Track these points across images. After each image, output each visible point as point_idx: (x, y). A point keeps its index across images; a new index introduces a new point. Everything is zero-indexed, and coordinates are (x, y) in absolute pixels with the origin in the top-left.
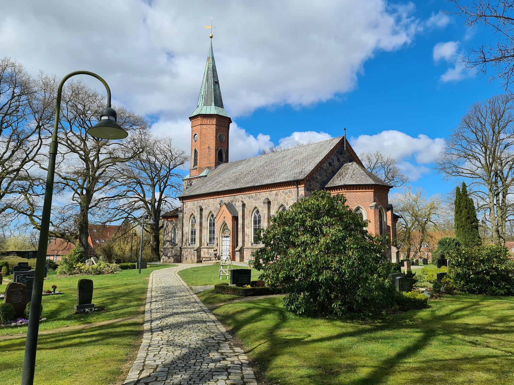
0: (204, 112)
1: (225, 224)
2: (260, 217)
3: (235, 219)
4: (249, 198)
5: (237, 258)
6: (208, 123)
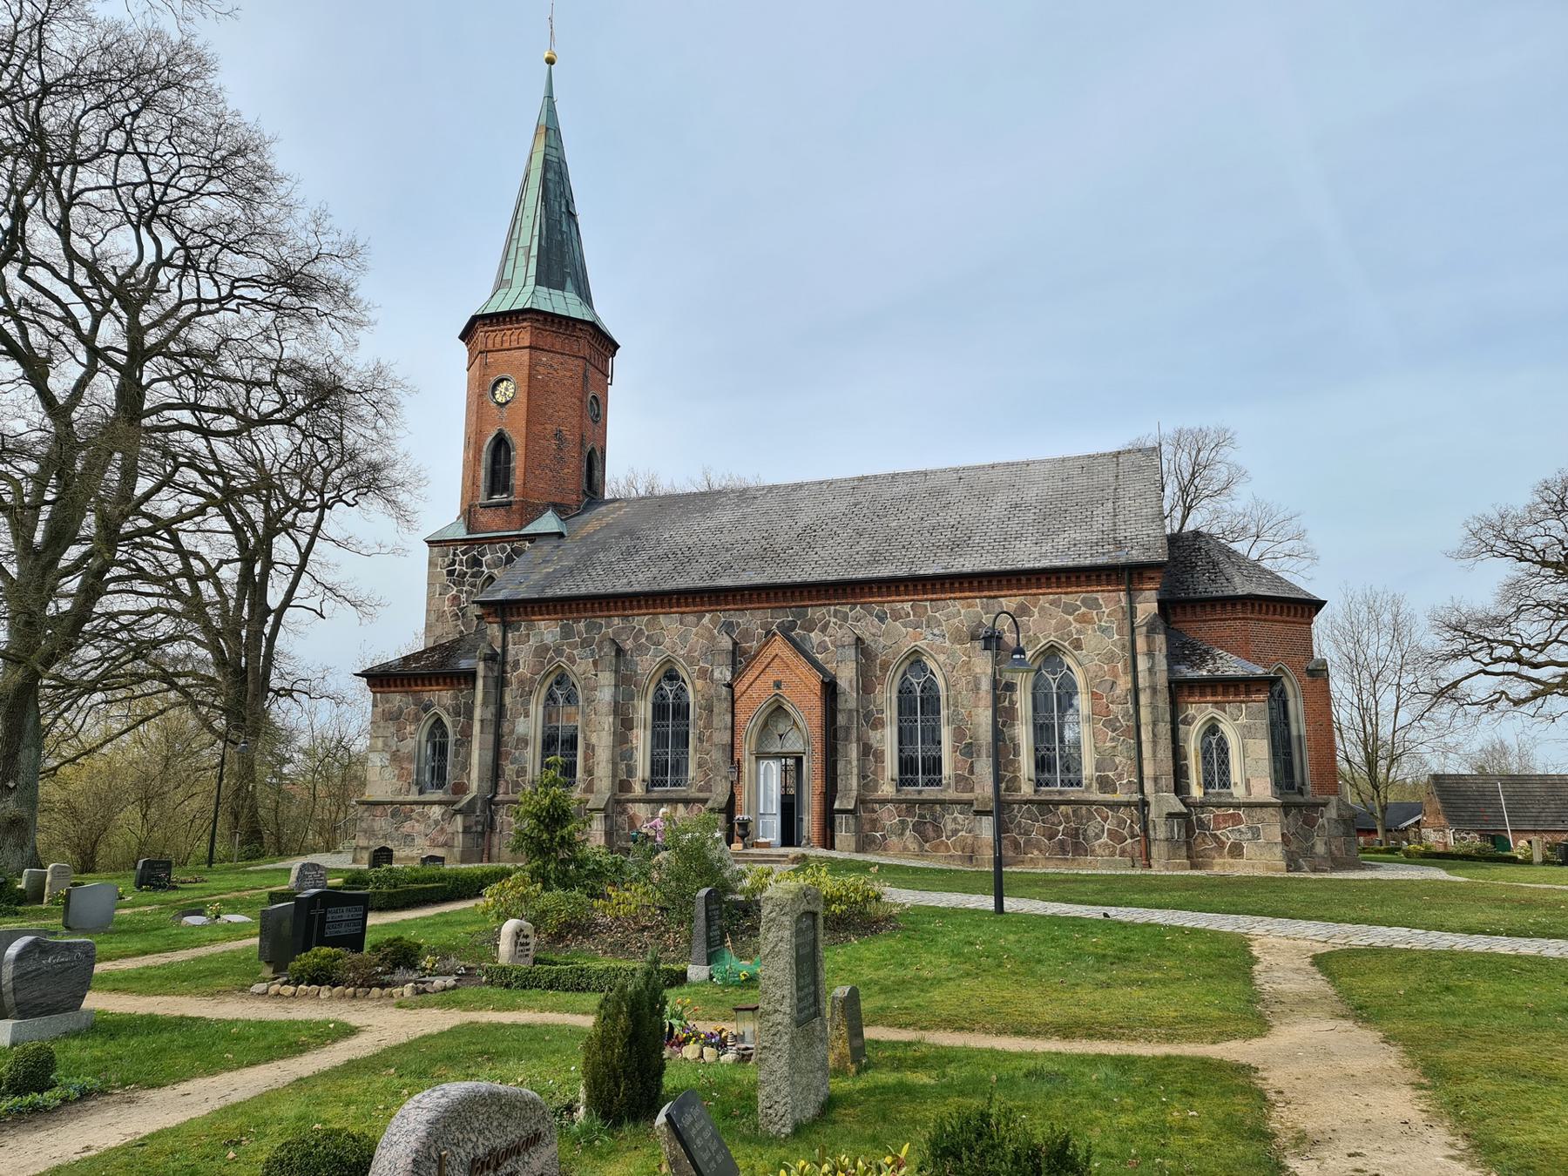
0: (546, 307)
1: (778, 711)
2: (930, 688)
3: (830, 689)
4: (882, 620)
5: (844, 836)
6: (558, 347)
